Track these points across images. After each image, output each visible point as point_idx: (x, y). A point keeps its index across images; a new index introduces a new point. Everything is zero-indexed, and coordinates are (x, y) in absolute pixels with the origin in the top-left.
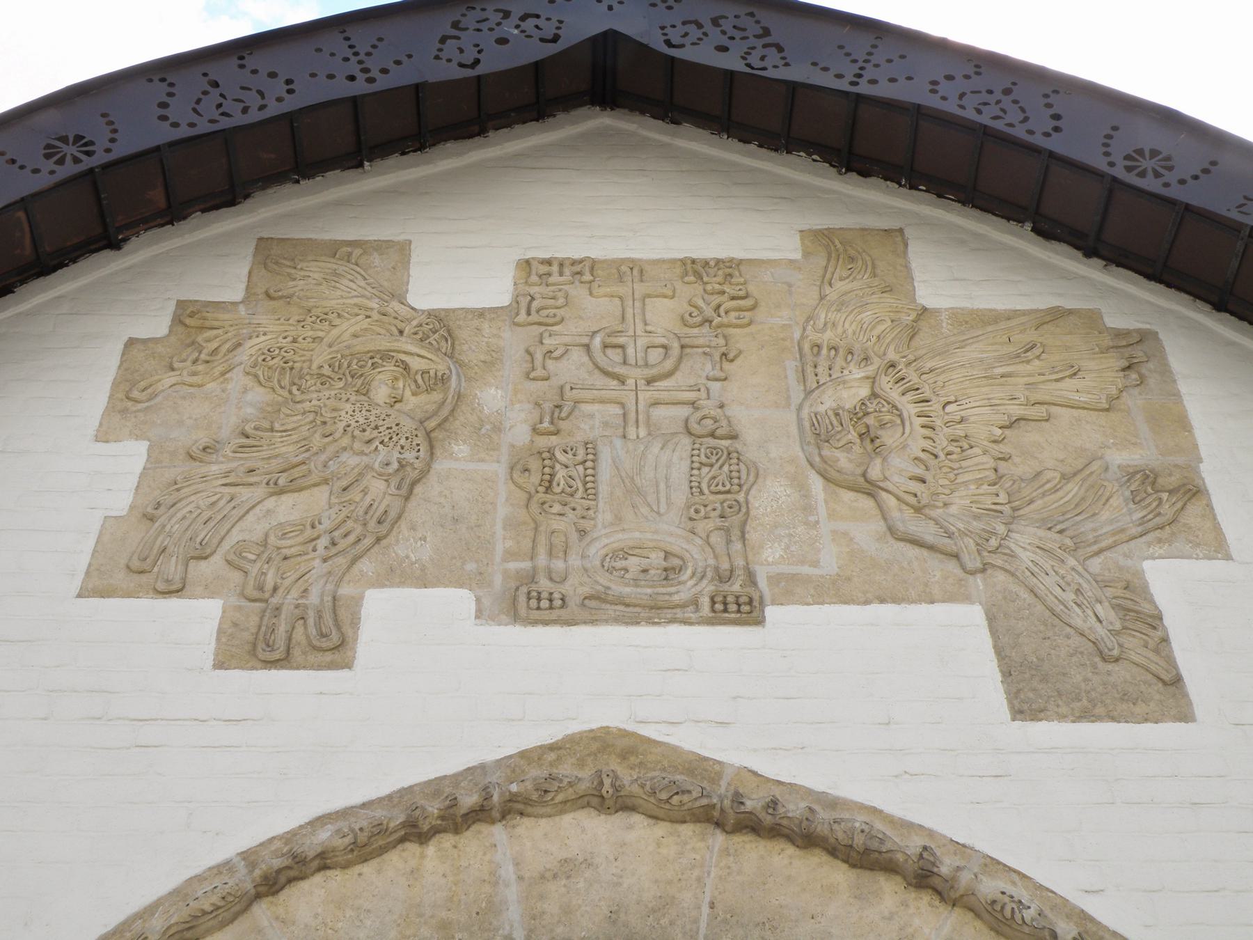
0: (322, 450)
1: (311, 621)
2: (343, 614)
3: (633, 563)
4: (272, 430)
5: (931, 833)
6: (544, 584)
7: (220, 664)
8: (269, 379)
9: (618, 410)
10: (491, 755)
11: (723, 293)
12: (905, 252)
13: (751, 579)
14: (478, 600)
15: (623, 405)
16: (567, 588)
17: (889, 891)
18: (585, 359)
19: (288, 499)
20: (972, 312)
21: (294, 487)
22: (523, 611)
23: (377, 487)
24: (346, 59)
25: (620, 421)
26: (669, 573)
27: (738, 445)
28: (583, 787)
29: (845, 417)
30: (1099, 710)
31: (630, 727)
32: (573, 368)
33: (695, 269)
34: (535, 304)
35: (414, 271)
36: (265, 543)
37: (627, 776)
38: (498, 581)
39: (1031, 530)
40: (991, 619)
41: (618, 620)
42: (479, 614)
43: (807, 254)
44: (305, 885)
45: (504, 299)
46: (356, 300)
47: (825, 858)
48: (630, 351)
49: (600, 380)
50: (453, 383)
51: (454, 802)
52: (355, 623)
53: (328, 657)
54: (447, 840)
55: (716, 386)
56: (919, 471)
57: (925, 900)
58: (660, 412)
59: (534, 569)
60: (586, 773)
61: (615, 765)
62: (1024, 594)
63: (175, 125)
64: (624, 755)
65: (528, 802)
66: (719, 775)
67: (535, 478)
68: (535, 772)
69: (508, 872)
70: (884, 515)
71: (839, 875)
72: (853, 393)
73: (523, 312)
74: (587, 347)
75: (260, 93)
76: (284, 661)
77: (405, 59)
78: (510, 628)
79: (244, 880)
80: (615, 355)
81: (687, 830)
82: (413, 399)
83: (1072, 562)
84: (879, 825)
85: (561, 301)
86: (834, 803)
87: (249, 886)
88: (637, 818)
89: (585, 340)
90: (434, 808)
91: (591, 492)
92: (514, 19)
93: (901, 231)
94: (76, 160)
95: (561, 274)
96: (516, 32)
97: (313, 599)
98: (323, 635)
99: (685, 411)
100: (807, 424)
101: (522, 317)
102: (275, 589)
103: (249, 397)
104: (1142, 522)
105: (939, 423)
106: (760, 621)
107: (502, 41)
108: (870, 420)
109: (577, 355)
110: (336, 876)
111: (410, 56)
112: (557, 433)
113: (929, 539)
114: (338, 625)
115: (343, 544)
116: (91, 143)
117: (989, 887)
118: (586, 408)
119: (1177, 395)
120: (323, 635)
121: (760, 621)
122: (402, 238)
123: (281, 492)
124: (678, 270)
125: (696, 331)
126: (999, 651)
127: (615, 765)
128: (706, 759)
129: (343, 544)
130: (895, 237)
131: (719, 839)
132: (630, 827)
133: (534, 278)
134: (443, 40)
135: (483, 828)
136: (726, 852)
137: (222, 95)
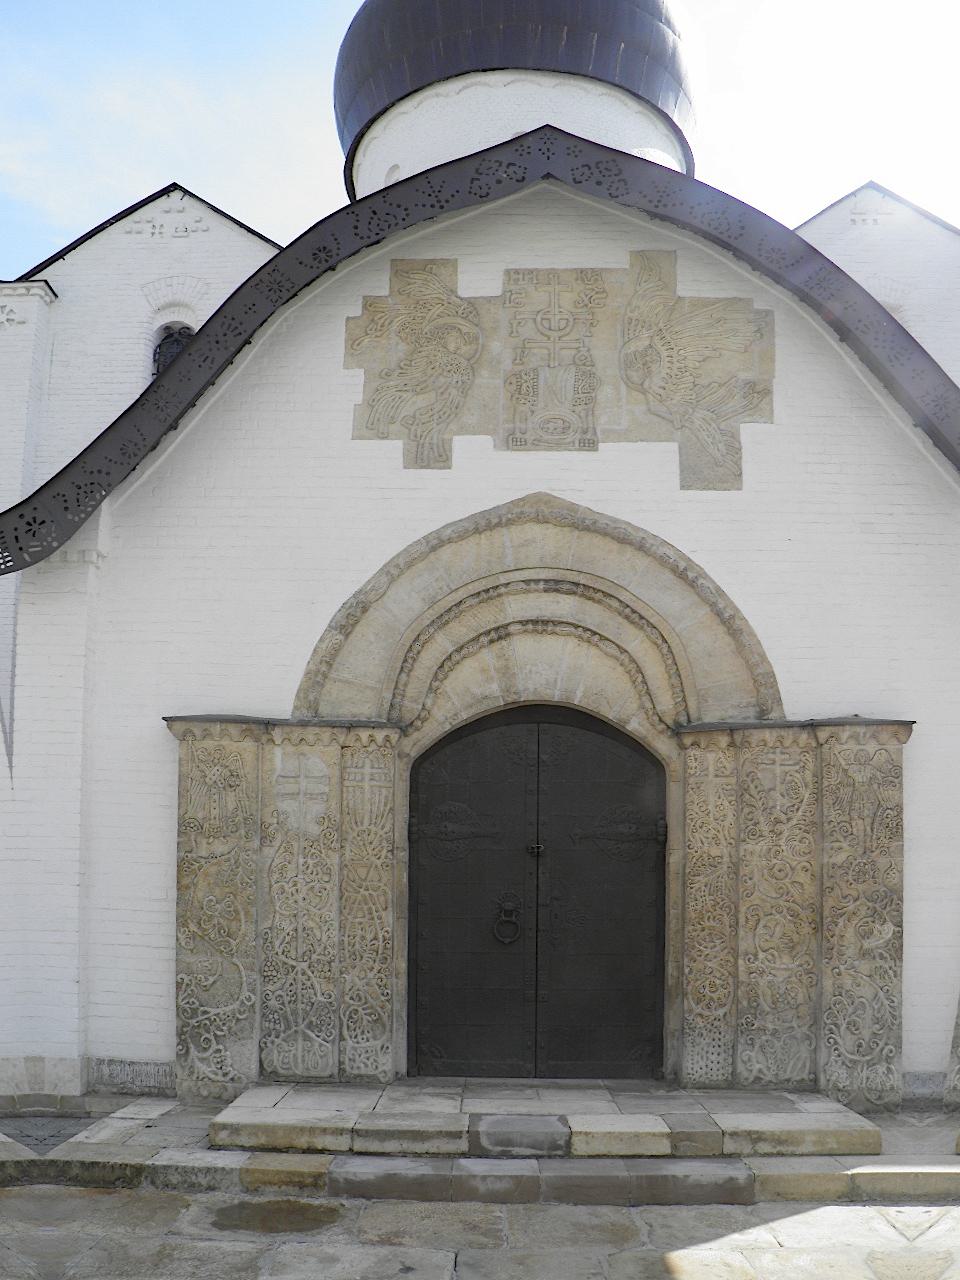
0: (432, 375)
1: (435, 450)
2: (447, 447)
3: (551, 426)
4: (411, 366)
5: (646, 531)
6: (518, 435)
7: (405, 468)
8: (406, 339)
9: (546, 351)
10: (501, 503)
11: (593, 290)
12: (675, 265)
13: (595, 433)
14: (494, 440)
15: (549, 349)
16: (527, 436)
17: (629, 551)
18: (534, 326)
19: (421, 397)
20: (699, 299)
21: (423, 391)
22: (511, 445)
23: (454, 392)
24: (430, 195)
25: (547, 357)
26: (565, 430)
27: (594, 370)
28: (532, 516)
29: (638, 356)
30: (711, 486)
31: (548, 492)
32: (528, 330)
33: (582, 274)
34: (513, 297)
35: (460, 276)
36: (414, 417)
37: (547, 511)
38: (501, 431)
39: (701, 412)
40: (680, 448)
41: (545, 450)
42: (495, 446)
43: (632, 265)
44: (444, 548)
45: (499, 292)
46: (437, 296)
47: (610, 540)
48: (552, 321)
49: (540, 337)
50: (480, 341)
51: (490, 522)
52: (451, 451)
53: (442, 464)
54: (488, 533)
55: (586, 340)
56: (663, 384)
57: (640, 554)
58: (564, 352)
59: (514, 428)
60: (533, 510)
61: (543, 507)
62: (694, 439)
63: (362, 238)
64: (546, 503)
65: (514, 521)
66: (576, 512)
67: (514, 387)
68: (517, 510)
69: (508, 544)
70: (648, 403)
71: (615, 546)
72: (640, 344)
73: (507, 302)
74: (535, 320)
75: (394, 216)
76: (427, 467)
77: (456, 194)
78: (505, 453)
79: (424, 548)
80: (546, 323)
81: (565, 529)
82: (465, 348)
83: (714, 425)
84: (630, 529)
85: (524, 295)
86: (616, 521)
87: (427, 549)
88: (550, 526)
89: (534, 317)
90: (483, 523)
91: (536, 394)
92: (504, 168)
93: (675, 251)
94: (327, 261)
95: (523, 280)
96: (505, 176)
97: (435, 441)
98: (441, 456)
99: (573, 352)
100: (622, 360)
101: (507, 305)
102: (421, 436)
103: (399, 347)
104: (746, 406)
105: (675, 360)
106: (597, 450)
107: (499, 182)
108: (648, 358)
109: (530, 324)
110: (454, 545)
111: (458, 192)
112: (523, 364)
113: (663, 415)
114: (445, 451)
115: (444, 418)
116: (330, 251)
117: (662, 550)
118: (536, 351)
119: (773, 344)
120: (441, 456)
121: (597, 450)
122: (453, 257)
123: (418, 394)
124: (575, 276)
125: (580, 310)
126: (681, 463)
127: (543, 507)
128: (574, 504)
129: (444, 418)
130: (672, 255)
131: (576, 533)
132: (548, 529)
133: (512, 282)
134: (473, 180)
135: (499, 528)
136: (578, 537)
137: (379, 219)
